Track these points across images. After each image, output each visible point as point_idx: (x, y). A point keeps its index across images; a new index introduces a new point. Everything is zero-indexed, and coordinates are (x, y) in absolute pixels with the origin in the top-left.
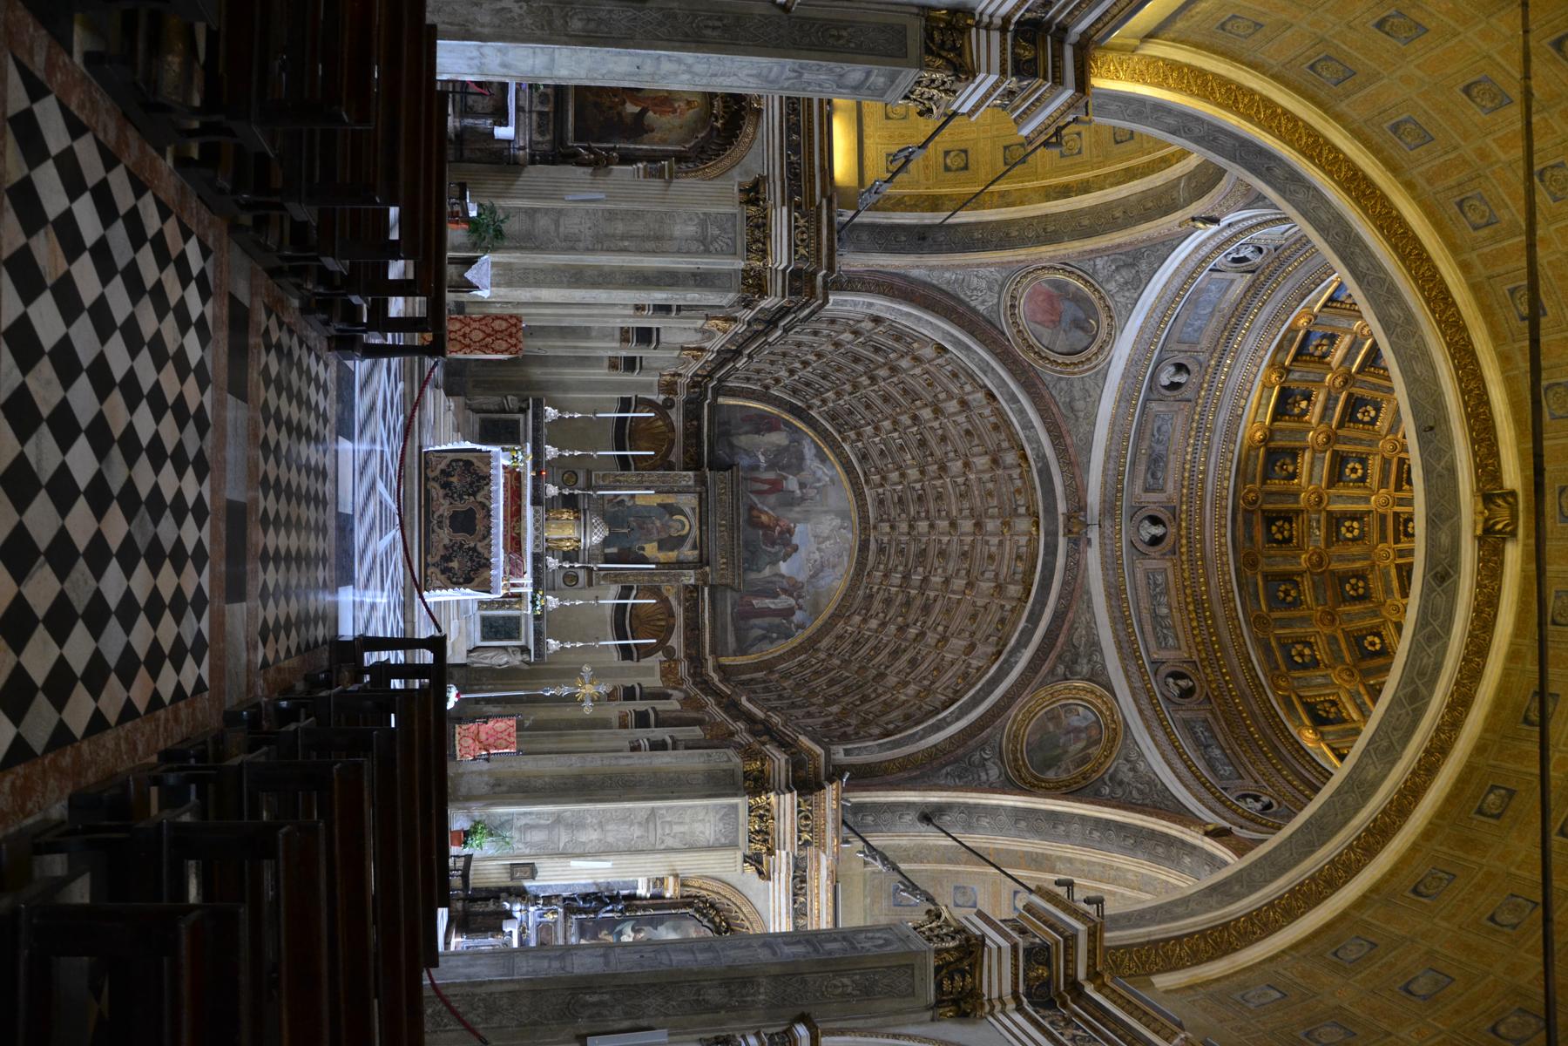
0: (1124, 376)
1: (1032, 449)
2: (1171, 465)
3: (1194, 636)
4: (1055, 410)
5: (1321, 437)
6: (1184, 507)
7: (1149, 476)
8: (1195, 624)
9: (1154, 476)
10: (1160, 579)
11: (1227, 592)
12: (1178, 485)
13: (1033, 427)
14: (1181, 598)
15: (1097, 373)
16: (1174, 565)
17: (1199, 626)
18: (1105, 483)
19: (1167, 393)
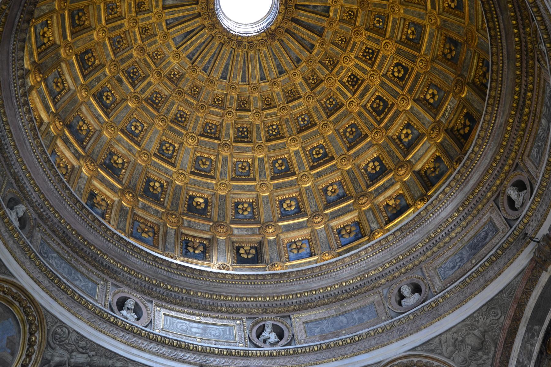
0: (418, 330)
1: (533, 345)
2: (472, 233)
3: (533, 83)
4: (498, 356)
5: (400, 173)
6: (489, 194)
7: (488, 240)
8: (529, 94)
9: (485, 238)
10: (535, 151)
11: (493, 106)
12: (481, 213)
13: (518, 361)
14: (530, 124)
15: (432, 351)
16: (523, 155)
17: (526, 91)
18: (507, 265)
19: (396, 291)
